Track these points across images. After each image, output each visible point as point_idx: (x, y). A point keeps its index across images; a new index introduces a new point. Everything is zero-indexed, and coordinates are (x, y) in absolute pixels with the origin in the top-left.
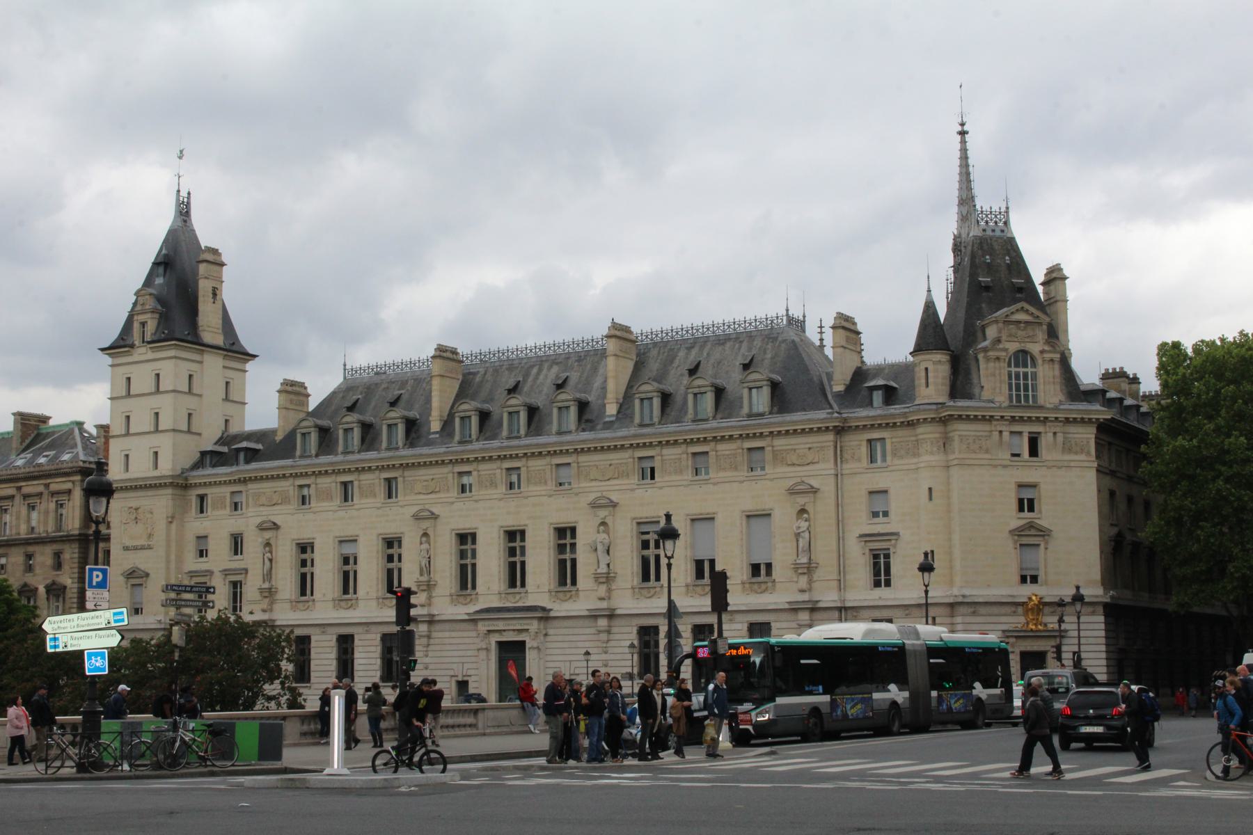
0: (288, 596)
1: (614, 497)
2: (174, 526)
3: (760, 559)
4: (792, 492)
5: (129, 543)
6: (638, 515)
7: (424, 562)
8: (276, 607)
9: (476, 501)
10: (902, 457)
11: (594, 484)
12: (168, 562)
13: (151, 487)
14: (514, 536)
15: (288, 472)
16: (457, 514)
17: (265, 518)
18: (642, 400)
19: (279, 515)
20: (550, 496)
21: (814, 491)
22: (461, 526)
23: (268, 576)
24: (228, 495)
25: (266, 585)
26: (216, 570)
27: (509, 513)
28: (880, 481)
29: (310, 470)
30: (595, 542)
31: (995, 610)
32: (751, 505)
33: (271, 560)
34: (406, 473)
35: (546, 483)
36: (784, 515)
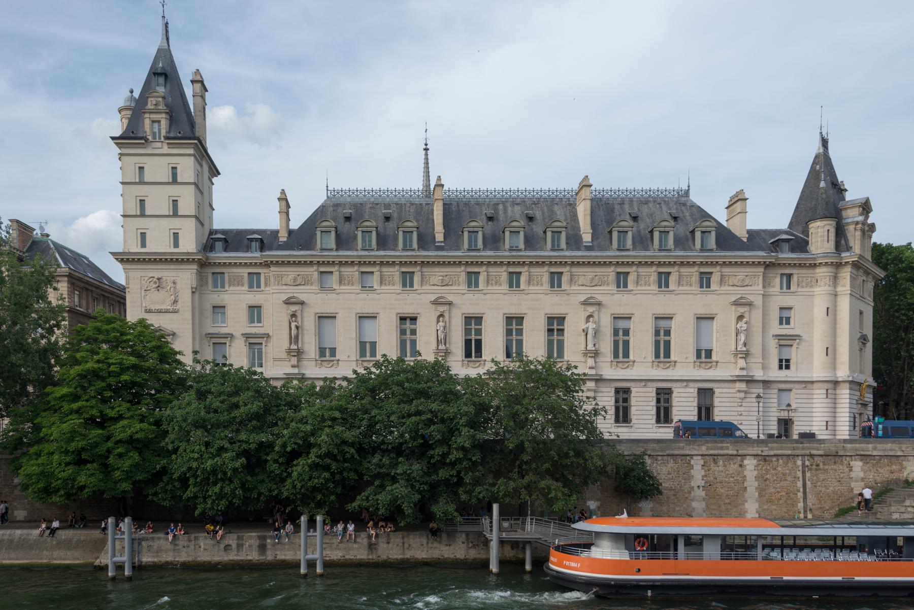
0: (313, 356)
1: (600, 298)
2: (197, 295)
3: (704, 346)
4: (736, 303)
5: (153, 308)
6: (616, 312)
7: (441, 336)
8: (305, 363)
9: (485, 294)
10: (803, 287)
11: (581, 288)
12: (193, 324)
13: (139, 261)
14: (514, 323)
15: (315, 260)
16: (467, 302)
17: (291, 295)
18: (703, 232)
19: (302, 293)
20: (546, 294)
21: (750, 304)
22: (471, 311)
23: (295, 339)
24: (246, 275)
25: (294, 347)
26: (237, 334)
27: (512, 304)
28: (787, 301)
29: (337, 260)
30: (588, 328)
31: (726, 385)
32: (702, 311)
33: (297, 327)
34: (424, 270)
35: (542, 285)
36: (726, 318)
